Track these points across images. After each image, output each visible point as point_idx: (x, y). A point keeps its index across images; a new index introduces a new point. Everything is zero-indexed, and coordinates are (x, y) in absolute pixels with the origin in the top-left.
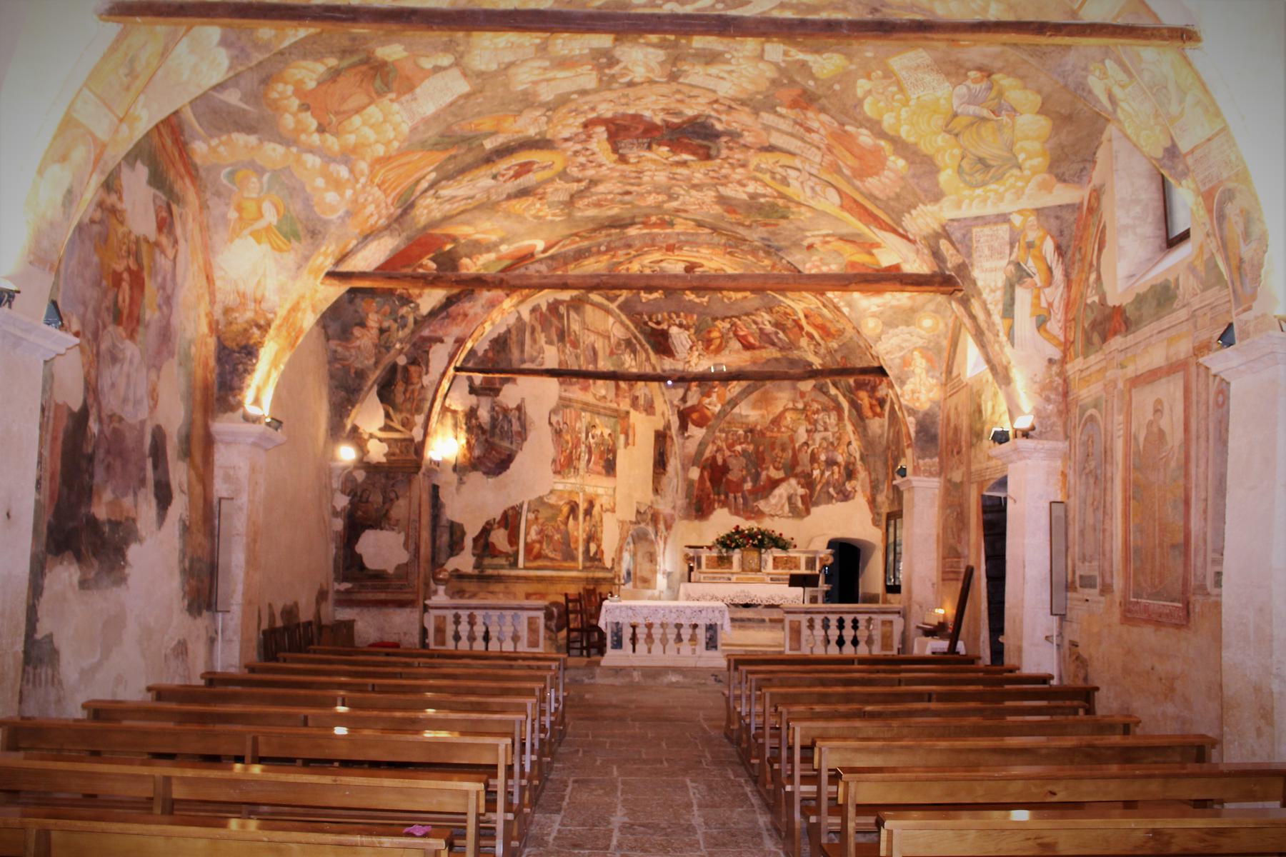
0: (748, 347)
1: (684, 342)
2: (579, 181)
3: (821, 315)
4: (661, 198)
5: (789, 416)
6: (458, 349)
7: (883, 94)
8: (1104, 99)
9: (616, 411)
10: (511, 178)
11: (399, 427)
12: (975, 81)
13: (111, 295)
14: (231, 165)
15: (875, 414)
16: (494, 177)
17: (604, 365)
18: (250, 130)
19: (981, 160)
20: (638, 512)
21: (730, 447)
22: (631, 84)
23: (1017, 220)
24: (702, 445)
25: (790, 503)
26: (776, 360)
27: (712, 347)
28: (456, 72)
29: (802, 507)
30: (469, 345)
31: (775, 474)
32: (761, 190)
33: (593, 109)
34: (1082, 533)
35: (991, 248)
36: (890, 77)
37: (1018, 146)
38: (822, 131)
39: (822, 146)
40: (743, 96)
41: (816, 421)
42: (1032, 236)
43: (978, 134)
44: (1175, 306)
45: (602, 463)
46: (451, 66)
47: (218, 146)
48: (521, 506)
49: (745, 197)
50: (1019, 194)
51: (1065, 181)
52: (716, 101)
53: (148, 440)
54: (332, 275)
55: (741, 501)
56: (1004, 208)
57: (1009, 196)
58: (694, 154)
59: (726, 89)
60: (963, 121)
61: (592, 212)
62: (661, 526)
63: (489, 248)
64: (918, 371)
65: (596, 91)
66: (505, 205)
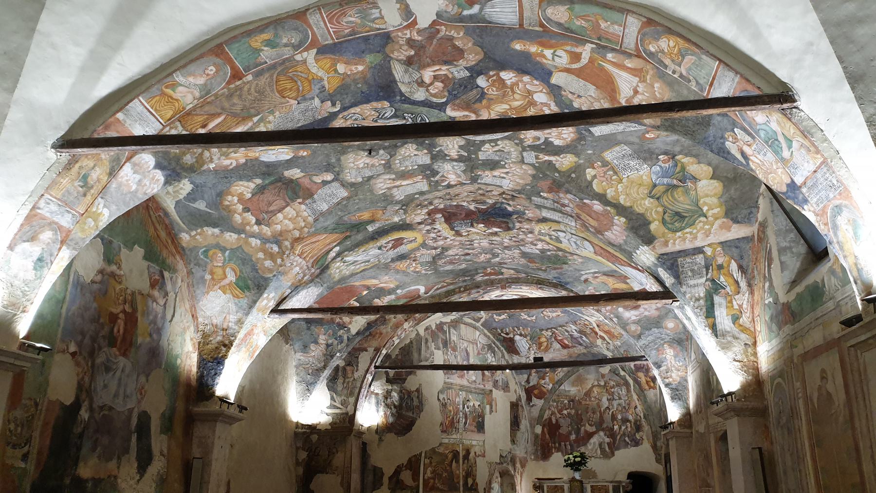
0: (565, 347)
1: (524, 345)
2: (435, 248)
3: (607, 325)
4: (488, 256)
5: (595, 390)
6: (376, 355)
7: (604, 177)
8: (739, 156)
9: (483, 390)
10: (391, 249)
11: (340, 406)
12: (664, 162)
13: (106, 329)
14: (205, 246)
15: (650, 387)
16: (380, 248)
17: (473, 361)
18: (214, 225)
19: (677, 214)
20: (501, 456)
21: (560, 411)
22: (449, 186)
23: (709, 251)
24: (542, 411)
25: (601, 448)
26: (584, 354)
27: (542, 348)
28: (336, 184)
29: (609, 451)
30: (384, 352)
31: (591, 429)
32: (546, 247)
33: (431, 203)
34: (785, 473)
35: (692, 271)
36: (607, 166)
37: (701, 202)
38: (571, 205)
39: (573, 215)
40: (519, 188)
41: (613, 393)
42: (720, 260)
43: (673, 196)
44: (824, 300)
45: (475, 424)
46: (333, 181)
47: (196, 235)
48: (421, 454)
49: (538, 252)
50: (707, 234)
51: (738, 222)
52: (504, 193)
53: (134, 421)
54: (276, 311)
55: (569, 447)
56: (698, 243)
57: (700, 235)
58: (499, 228)
59: (507, 184)
60: (660, 189)
61: (449, 267)
62: (518, 465)
63: (391, 292)
64: (668, 357)
65: (429, 192)
66: (393, 265)
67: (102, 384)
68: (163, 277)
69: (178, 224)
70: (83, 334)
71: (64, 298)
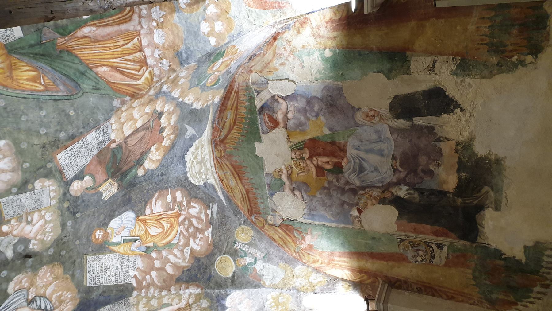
67: (375, 174)
68: (262, 107)
69: (213, 112)
70: (343, 204)
71: (324, 226)
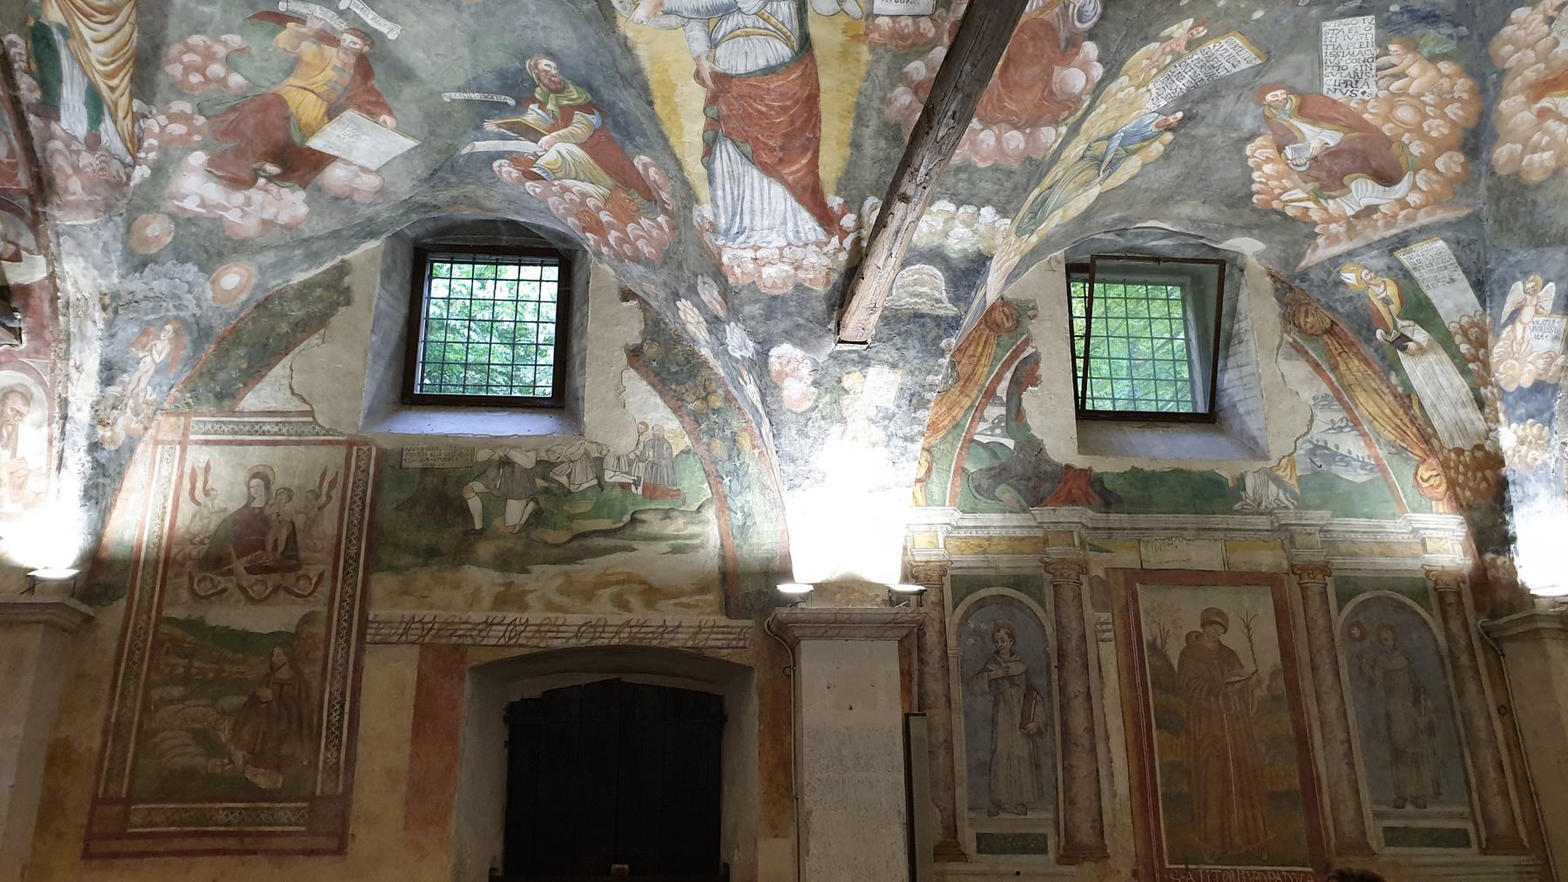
8: (1508, 309)
